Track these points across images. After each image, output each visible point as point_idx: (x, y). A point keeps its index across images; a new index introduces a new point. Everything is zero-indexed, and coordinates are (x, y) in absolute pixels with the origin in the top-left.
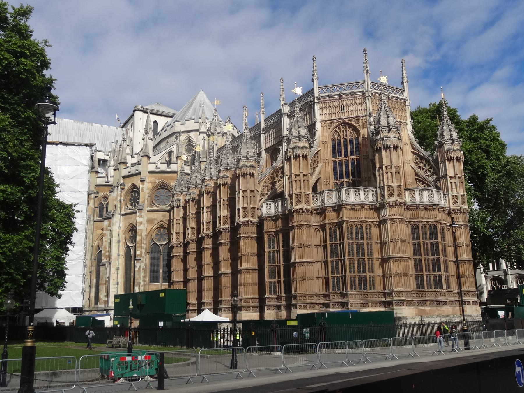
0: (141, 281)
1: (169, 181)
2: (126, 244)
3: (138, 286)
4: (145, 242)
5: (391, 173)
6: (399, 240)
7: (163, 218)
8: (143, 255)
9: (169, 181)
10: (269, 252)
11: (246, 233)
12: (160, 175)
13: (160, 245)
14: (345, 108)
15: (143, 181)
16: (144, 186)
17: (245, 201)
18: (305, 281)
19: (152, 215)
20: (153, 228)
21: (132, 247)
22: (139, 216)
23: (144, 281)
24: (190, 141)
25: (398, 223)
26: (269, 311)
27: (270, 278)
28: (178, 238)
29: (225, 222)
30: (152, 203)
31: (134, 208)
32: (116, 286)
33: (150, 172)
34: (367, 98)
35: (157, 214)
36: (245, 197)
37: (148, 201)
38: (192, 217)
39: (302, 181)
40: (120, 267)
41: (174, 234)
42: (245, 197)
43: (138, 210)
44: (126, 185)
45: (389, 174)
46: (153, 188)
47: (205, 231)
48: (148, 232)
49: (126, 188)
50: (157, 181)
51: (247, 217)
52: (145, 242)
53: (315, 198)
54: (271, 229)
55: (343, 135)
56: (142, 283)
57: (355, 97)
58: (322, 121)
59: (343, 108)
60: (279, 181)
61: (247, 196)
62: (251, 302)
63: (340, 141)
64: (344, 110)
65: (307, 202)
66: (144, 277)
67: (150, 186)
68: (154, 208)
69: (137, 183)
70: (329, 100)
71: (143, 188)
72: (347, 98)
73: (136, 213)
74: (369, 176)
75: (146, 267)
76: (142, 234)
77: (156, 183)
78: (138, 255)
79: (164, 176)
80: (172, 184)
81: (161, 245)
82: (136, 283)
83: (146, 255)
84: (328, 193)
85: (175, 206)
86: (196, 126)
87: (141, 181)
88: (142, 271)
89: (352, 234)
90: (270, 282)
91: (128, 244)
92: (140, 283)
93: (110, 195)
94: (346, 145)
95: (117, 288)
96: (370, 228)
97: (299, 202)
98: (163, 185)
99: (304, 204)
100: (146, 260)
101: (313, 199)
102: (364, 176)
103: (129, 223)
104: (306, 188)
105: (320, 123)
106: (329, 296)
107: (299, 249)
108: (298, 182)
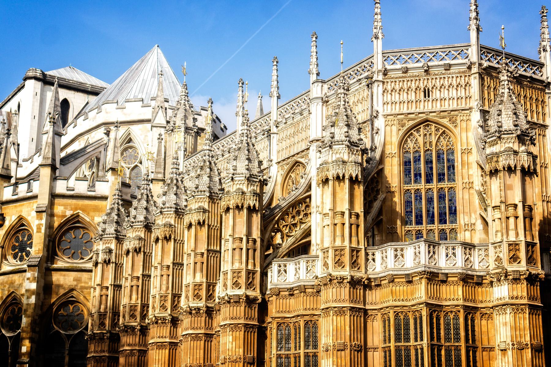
1: (92, 214)
4: (37, 329)
5: (517, 217)
6: (529, 346)
7: (75, 283)
9: (92, 214)
10: (279, 357)
11: (236, 318)
12: (74, 201)
14: (430, 93)
17: (237, 257)
22: (28, 279)
24: (130, 140)
25: (527, 312)
29: (197, 296)
31: (19, 263)
35: (64, 276)
38: (133, 284)
42: (237, 251)
43: (29, 266)
45: (512, 220)
47: (157, 311)
50: (69, 213)
51: (240, 288)
52: (37, 329)
53: (370, 257)
57: (449, 74)
58: (388, 115)
59: (427, 93)
60: (302, 223)
64: (429, 97)
69: (29, 215)
70: (402, 77)
74: (473, 221)
77: (66, 216)
79: (82, 205)
81: (69, 336)
84: (396, 250)
85: (100, 260)
86: (147, 114)
87: (37, 212)
89: (438, 329)
96: (473, 321)
97: (339, 263)
99: (347, 268)
102: (462, 223)
104: (354, 239)
105: (384, 120)
107: (339, 353)
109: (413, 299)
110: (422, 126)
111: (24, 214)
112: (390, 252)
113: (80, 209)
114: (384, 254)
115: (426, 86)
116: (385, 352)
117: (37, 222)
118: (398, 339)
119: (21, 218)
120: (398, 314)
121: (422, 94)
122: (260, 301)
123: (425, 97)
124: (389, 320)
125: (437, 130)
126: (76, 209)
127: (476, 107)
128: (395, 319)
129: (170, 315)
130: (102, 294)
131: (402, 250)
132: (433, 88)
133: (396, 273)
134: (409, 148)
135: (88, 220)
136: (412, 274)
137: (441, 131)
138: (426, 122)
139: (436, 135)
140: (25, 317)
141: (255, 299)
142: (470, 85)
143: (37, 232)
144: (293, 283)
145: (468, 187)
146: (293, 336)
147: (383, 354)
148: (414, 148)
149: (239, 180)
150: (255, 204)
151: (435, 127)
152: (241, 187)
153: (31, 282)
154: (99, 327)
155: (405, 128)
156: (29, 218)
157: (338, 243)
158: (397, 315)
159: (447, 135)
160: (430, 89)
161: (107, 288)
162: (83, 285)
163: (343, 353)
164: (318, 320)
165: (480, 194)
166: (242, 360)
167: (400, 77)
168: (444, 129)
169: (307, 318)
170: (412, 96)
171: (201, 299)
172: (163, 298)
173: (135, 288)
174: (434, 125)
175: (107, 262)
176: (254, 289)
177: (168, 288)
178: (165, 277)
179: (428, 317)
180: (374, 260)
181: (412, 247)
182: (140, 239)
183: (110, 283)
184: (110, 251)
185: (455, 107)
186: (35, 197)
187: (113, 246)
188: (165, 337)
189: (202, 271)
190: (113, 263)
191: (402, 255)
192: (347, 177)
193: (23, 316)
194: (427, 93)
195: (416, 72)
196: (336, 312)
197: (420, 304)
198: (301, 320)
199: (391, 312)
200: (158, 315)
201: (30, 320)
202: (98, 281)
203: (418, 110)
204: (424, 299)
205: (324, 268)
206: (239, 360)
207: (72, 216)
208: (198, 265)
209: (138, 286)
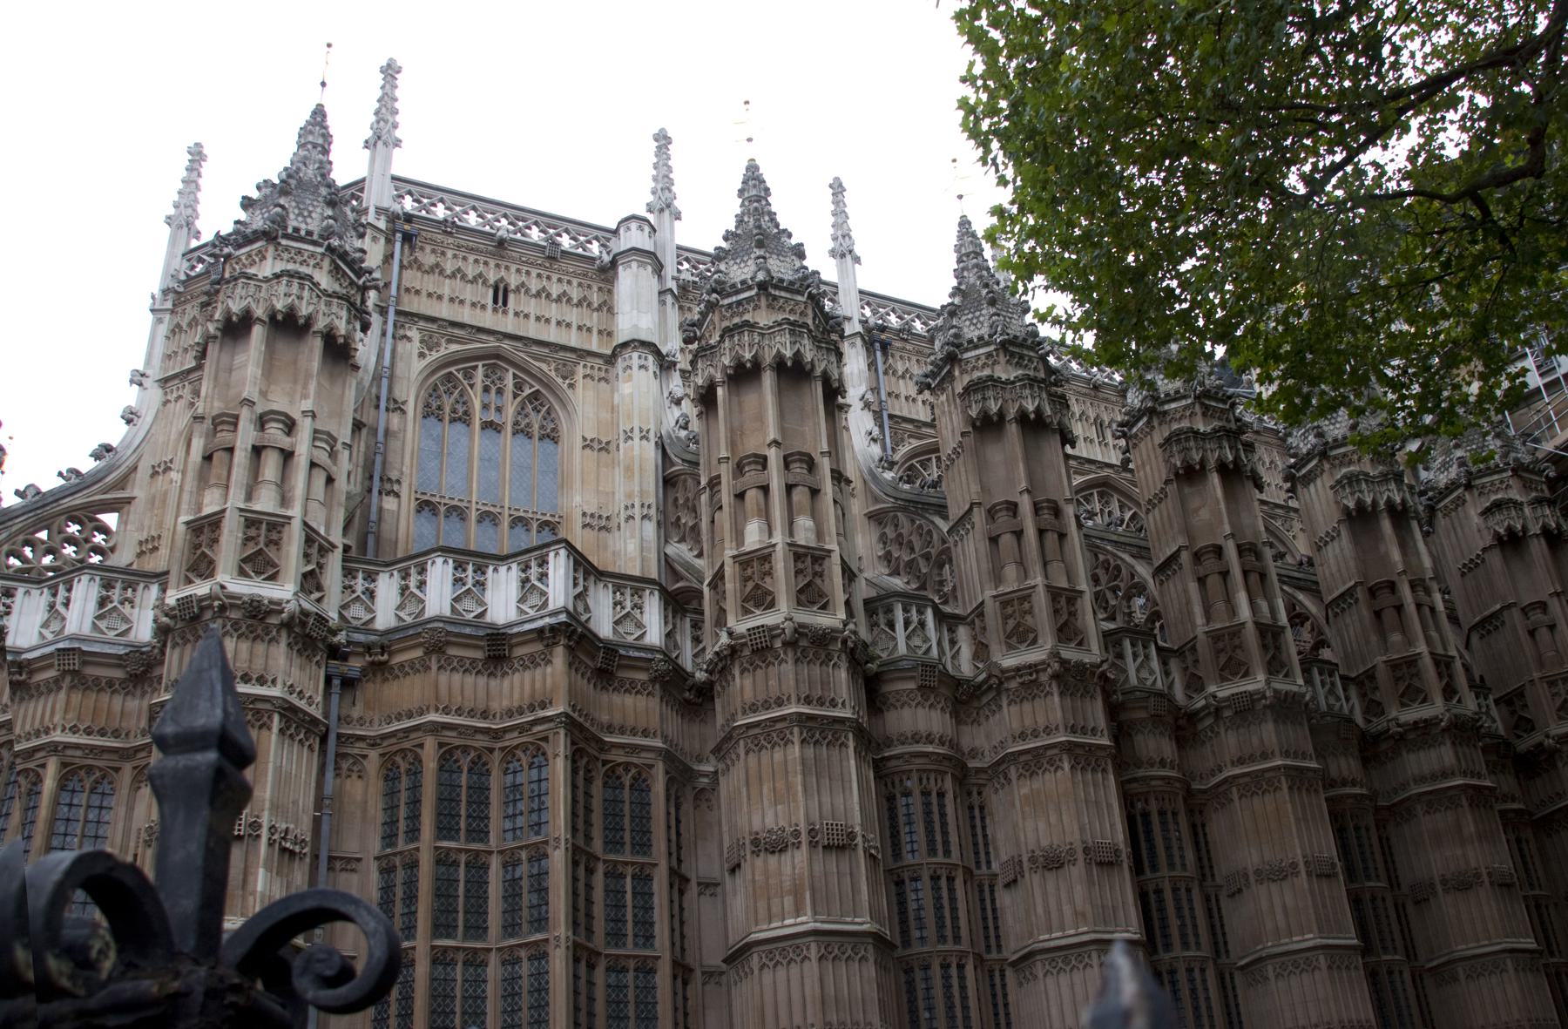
14: (511, 297)
59: (501, 294)
64: (505, 303)
110: (480, 364)
115: (502, 279)
120: (450, 752)
121: (491, 292)
123: (495, 301)
124: (415, 772)
125: (519, 386)
128: (441, 768)
137: (528, 391)
138: (495, 360)
139: (515, 396)
155: (435, 355)
158: (447, 756)
174: (511, 371)
179: (569, 762)
181: (514, 566)
191: (481, 585)
194: (501, 294)
199: (427, 746)
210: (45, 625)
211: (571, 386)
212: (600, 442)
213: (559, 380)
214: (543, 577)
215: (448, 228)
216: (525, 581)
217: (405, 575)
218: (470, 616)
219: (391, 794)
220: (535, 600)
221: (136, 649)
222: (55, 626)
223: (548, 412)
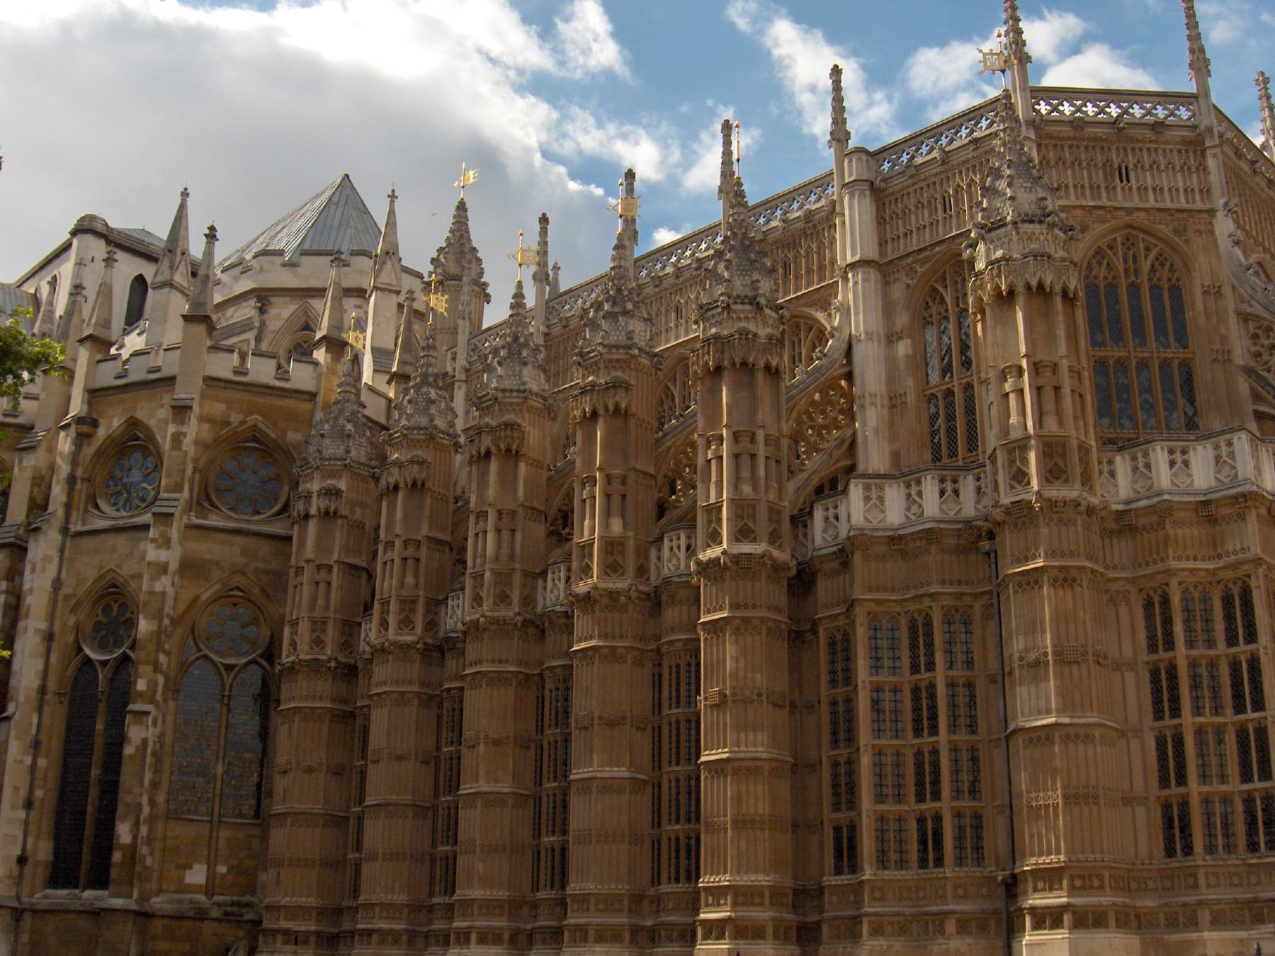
0: (145, 800)
2: (80, 650)
3: (132, 819)
7: (244, 560)
8: (159, 697)
12: (247, 397)
13: (224, 665)
15: (181, 411)
16: (185, 429)
17: (745, 474)
18: (1095, 809)
19: (204, 549)
20: (204, 597)
21: (104, 663)
22: (153, 541)
23: (152, 802)
26: (881, 942)
27: (880, 798)
28: (318, 643)
30: (205, 499)
31: (124, 514)
32: (22, 814)
33: (211, 381)
34: (1208, 152)
36: (745, 460)
37: (191, 489)
39: (1066, 390)
40: (44, 739)
41: (304, 628)
42: (745, 460)
43: (154, 514)
44: (103, 422)
46: (217, 442)
48: (181, 608)
49: (102, 433)
50: (235, 418)
51: (754, 540)
54: (885, 590)
55: (1126, 271)
56: (146, 810)
57: (1166, 143)
59: (1124, 175)
61: (753, 456)
62: (767, 900)
63: (1112, 288)
64: (1128, 181)
65: (1086, 479)
66: (155, 785)
67: (206, 431)
68: (214, 520)
70: (1074, 138)
71: (177, 439)
72: (1142, 141)
73: (146, 527)
75: (161, 747)
76: (161, 610)
77: (227, 424)
78: (141, 695)
80: (293, 436)
81: (229, 668)
82: (120, 809)
83: (165, 701)
84: (1171, 452)
88: (149, 759)
90: (882, 819)
91: (88, 651)
92: (139, 806)
93: (21, 461)
94: (1136, 309)
95: (26, 822)
98: (254, 439)
99: (1078, 485)
100: (164, 721)
101: (1101, 473)
103: (101, 567)
106: (1195, 876)
108: (1048, 394)
109: (1220, 557)
111: (141, 415)
112: (1159, 456)
113: (259, 413)
114: (1141, 460)
116: (1155, 673)
117: (172, 429)
118: (1190, 643)
119: (133, 423)
122: (794, 572)
123: (1121, 181)
124: (1165, 601)
125: (1147, 249)
126: (251, 413)
127: (1222, 209)
129: (519, 614)
130: (318, 578)
131: (1184, 452)
132: (1136, 166)
133: (1176, 498)
134: (1095, 277)
135: (273, 436)
136: (1218, 500)
140: (144, 618)
141: (785, 567)
142: (1204, 169)
143: (173, 448)
144: (902, 527)
145: (1220, 358)
146: (905, 643)
147: (1147, 677)
148: (1105, 278)
149: (742, 311)
150: (777, 365)
151: (1144, 240)
152: (743, 324)
153: (159, 547)
154: (311, 648)
156: (152, 423)
157: (1051, 425)
159: (1166, 260)
160: (1131, 166)
161: (330, 568)
162: (260, 565)
163: (1075, 668)
164: (971, 607)
165: (1249, 371)
166: (764, 698)
167: (1069, 138)
168: (1161, 246)
169: (947, 601)
170: (1099, 177)
171: (623, 574)
172: (503, 579)
173: (410, 562)
174: (1141, 236)
175: (328, 516)
176: (780, 546)
177: (512, 557)
178: (506, 534)
180: (1112, 474)
182: (422, 463)
183: (335, 557)
184: (337, 493)
185: (1183, 204)
186: (171, 380)
187: (343, 485)
188: (507, 662)
189: (623, 516)
190: (342, 517)
191: (1186, 464)
192: (1058, 288)
193: (141, 617)
195: (1100, 131)
196: (1056, 580)
197: (1242, 563)
198: (934, 605)
200: (490, 614)
201: (153, 626)
202: (309, 552)
203: (1108, 203)
204: (1256, 550)
205: (1014, 484)
206: (755, 697)
207: (242, 423)
208: (616, 499)
209: (418, 560)
210: (908, 509)
211: (1187, 242)
212: (1214, 287)
213: (1176, 239)
214: (1232, 455)
215: (1078, 124)
216: (1218, 459)
217: (1134, 459)
218: (1183, 486)
219: (1149, 617)
220: (1226, 470)
221: (967, 522)
222: (914, 509)
223: (1172, 265)
